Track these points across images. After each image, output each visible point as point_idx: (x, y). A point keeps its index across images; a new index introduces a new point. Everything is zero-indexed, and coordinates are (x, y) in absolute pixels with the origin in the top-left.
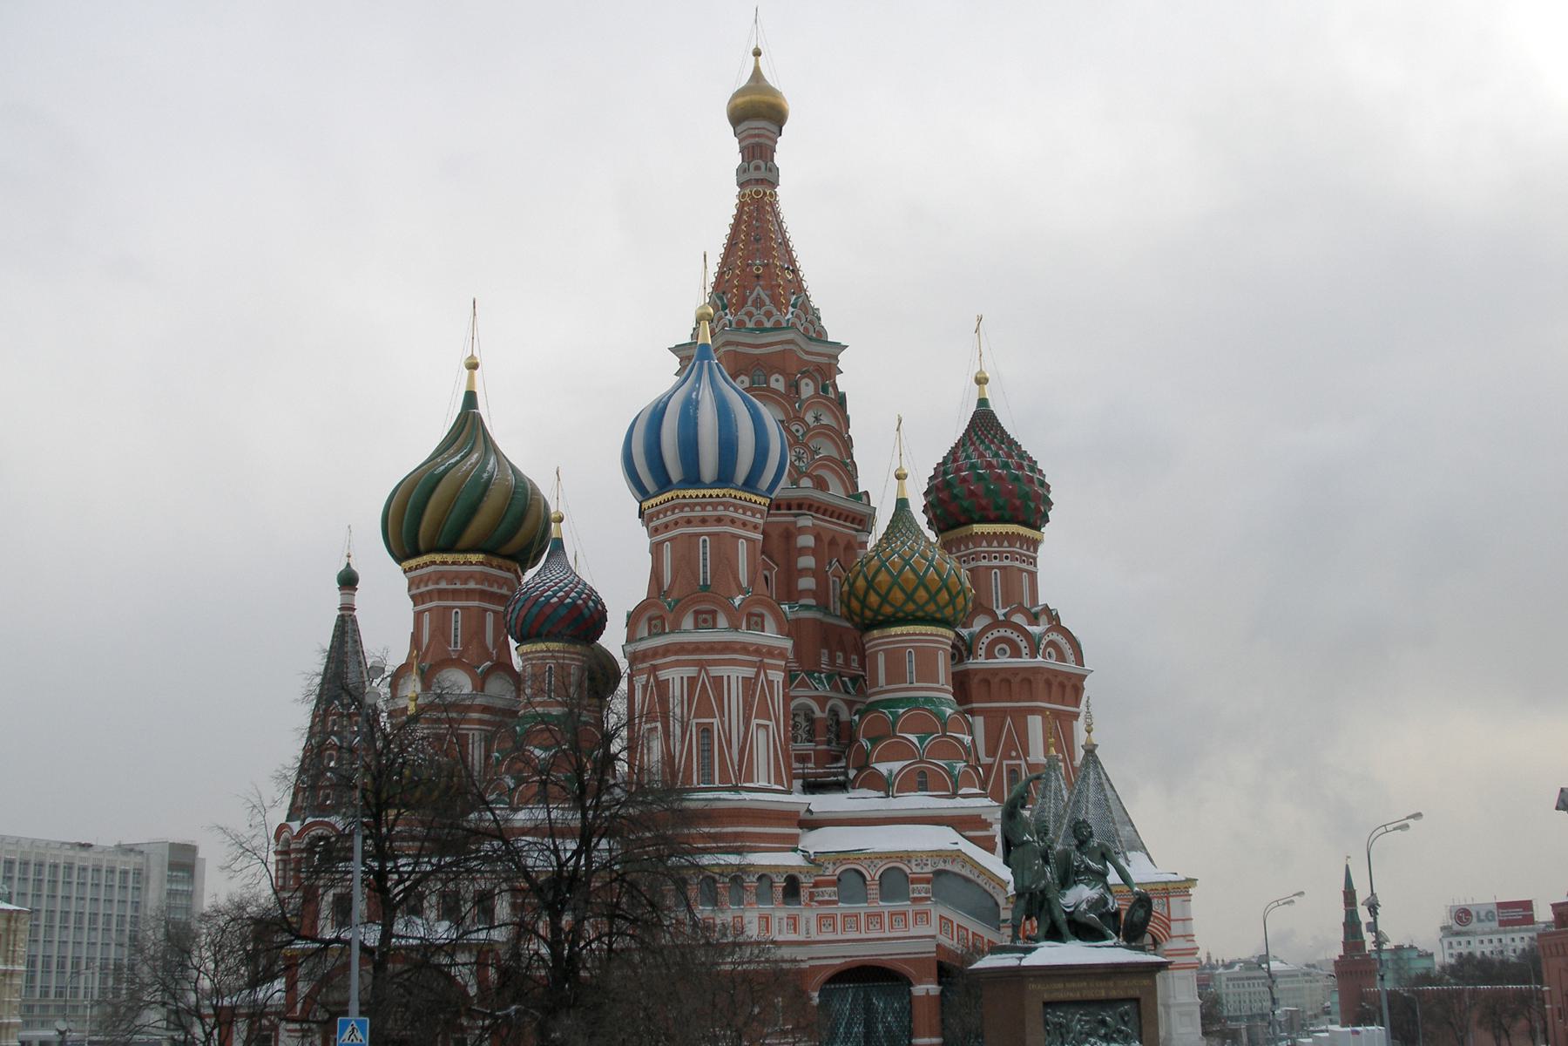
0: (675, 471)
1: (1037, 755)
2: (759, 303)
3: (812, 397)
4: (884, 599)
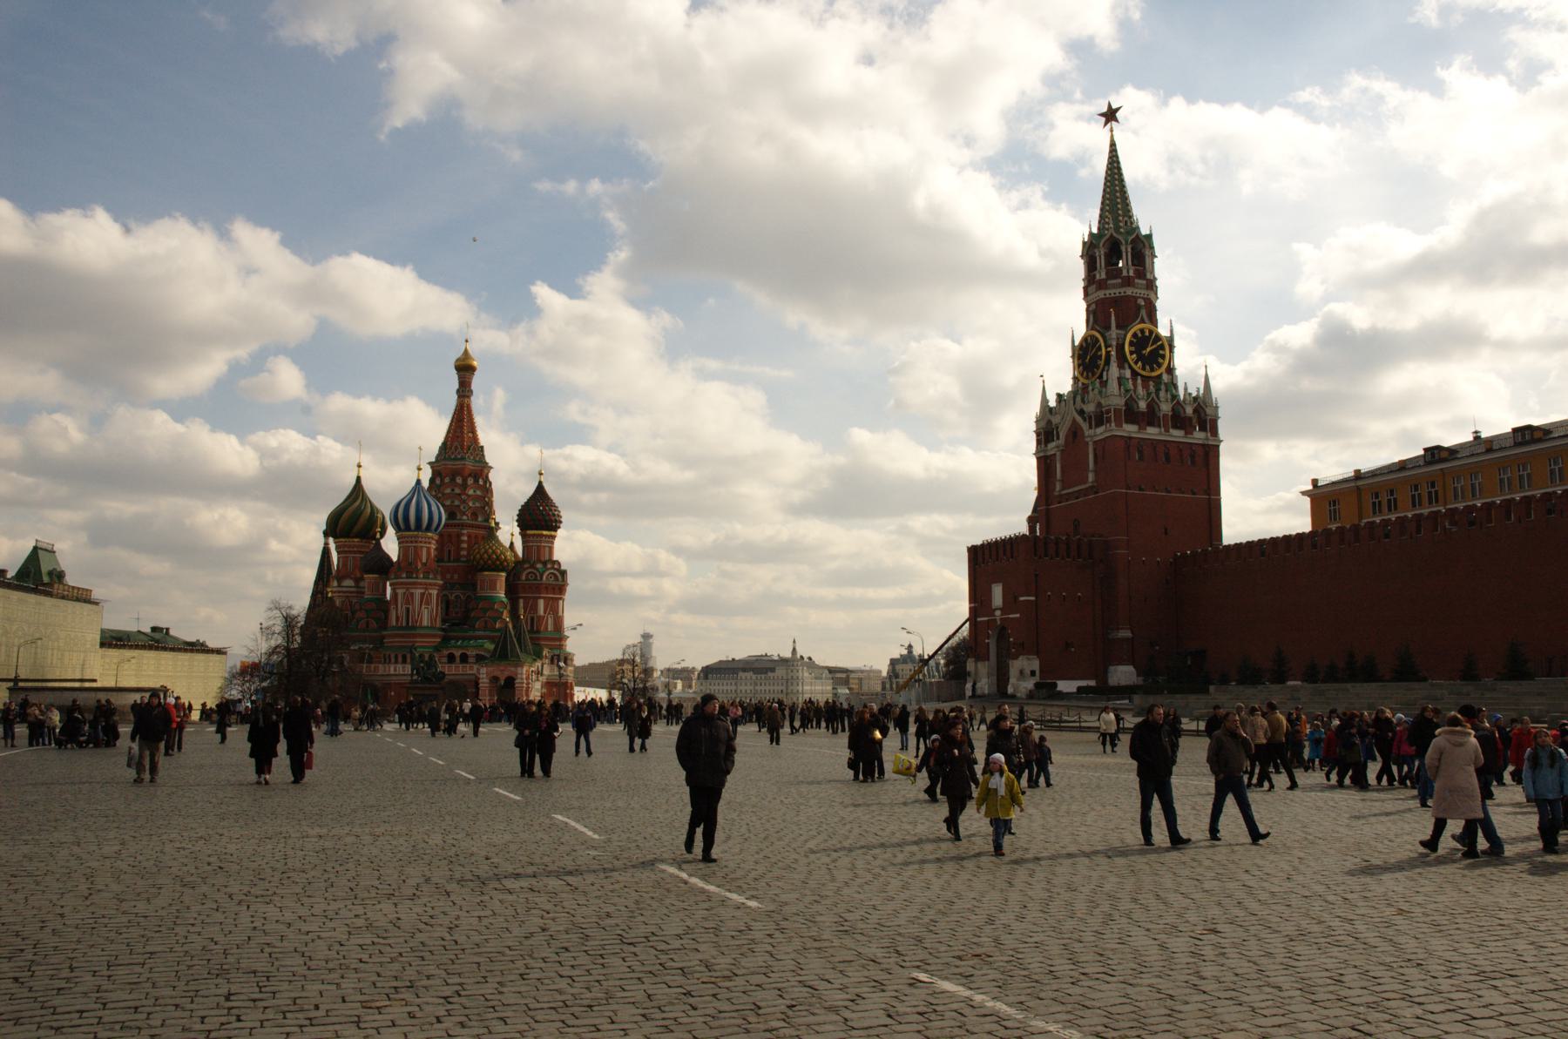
1: (541, 612)
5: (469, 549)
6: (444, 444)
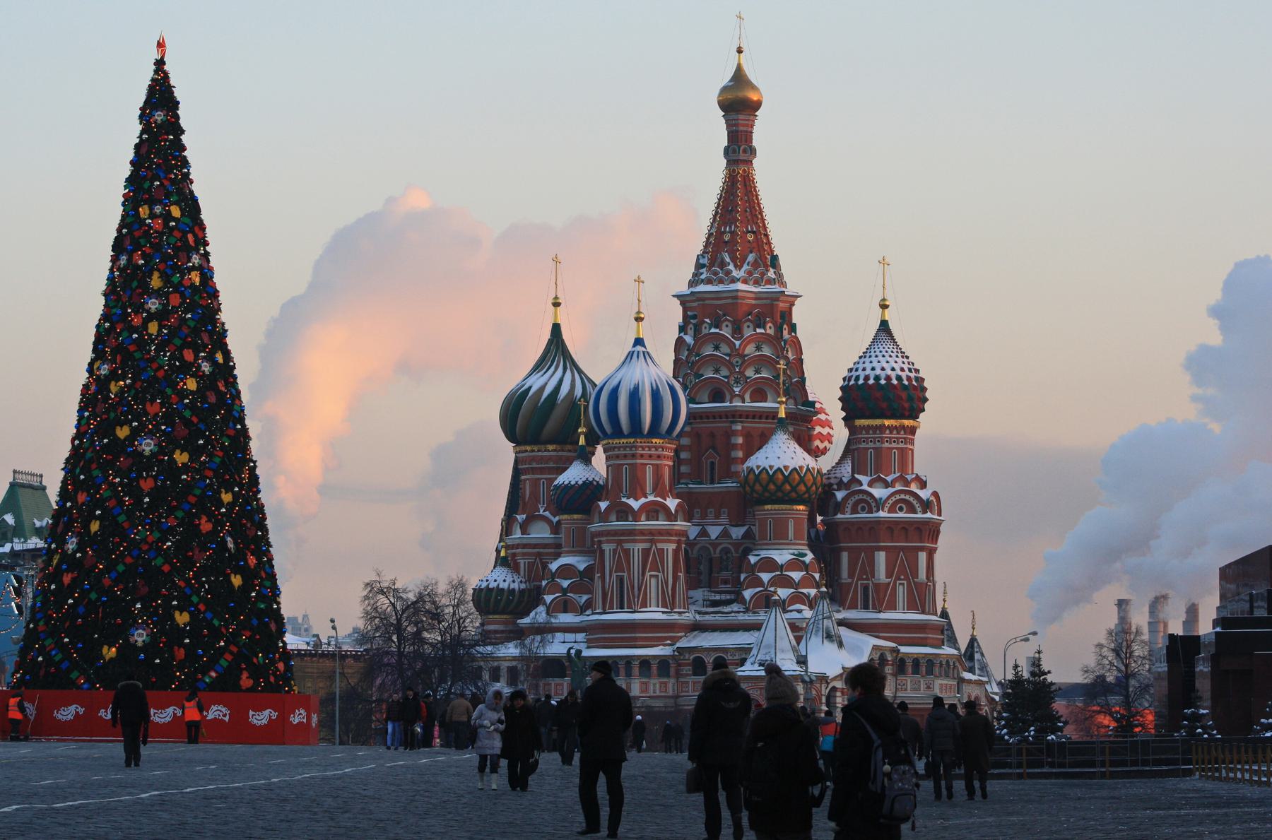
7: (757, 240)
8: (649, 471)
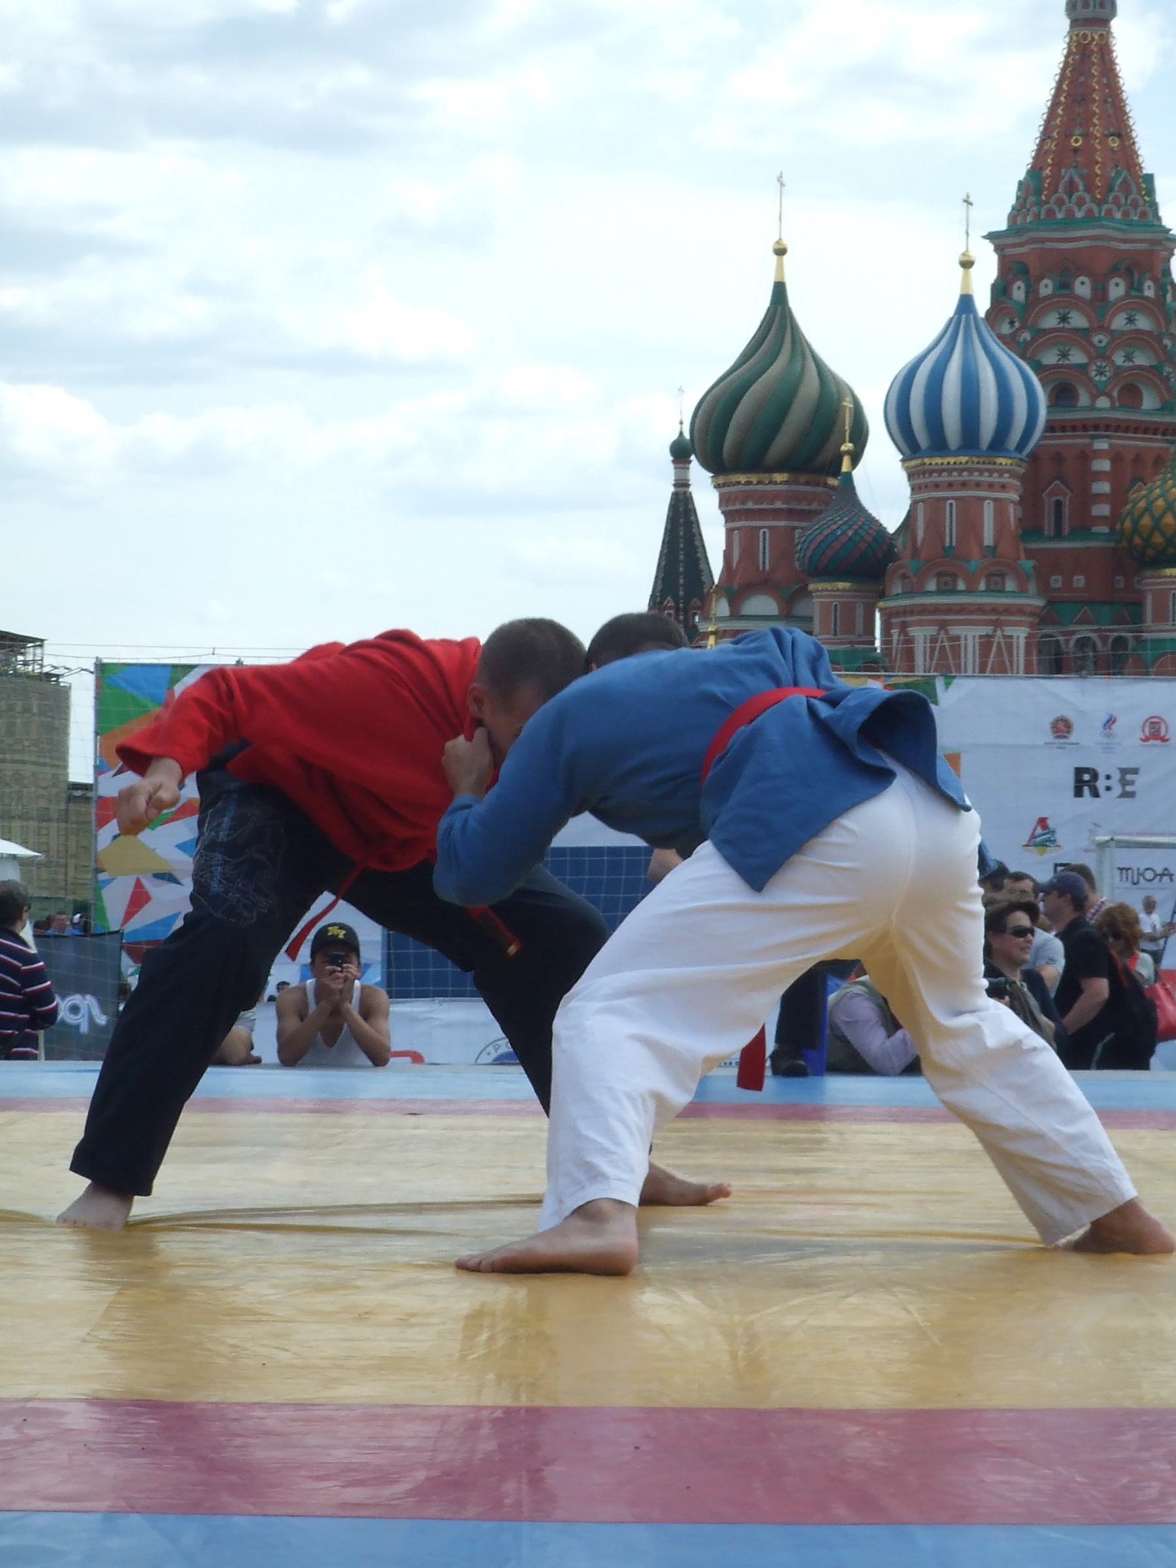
0: (922, 438)
2: (1071, 188)
3: (1121, 299)
4: (1147, 541)
5: (1118, 499)
6: (1035, 170)
7: (1122, 145)
8: (988, 510)
